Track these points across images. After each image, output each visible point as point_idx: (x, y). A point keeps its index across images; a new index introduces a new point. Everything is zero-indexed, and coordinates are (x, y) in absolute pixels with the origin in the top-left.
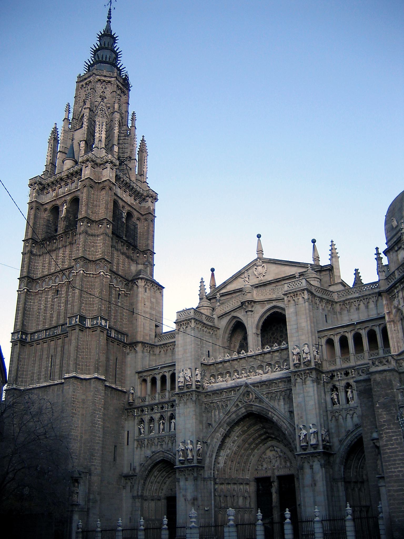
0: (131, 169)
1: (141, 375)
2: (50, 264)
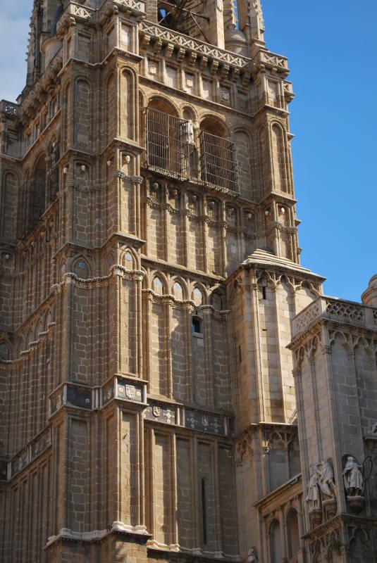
0: (208, 20)
1: (265, 511)
2: (38, 289)
